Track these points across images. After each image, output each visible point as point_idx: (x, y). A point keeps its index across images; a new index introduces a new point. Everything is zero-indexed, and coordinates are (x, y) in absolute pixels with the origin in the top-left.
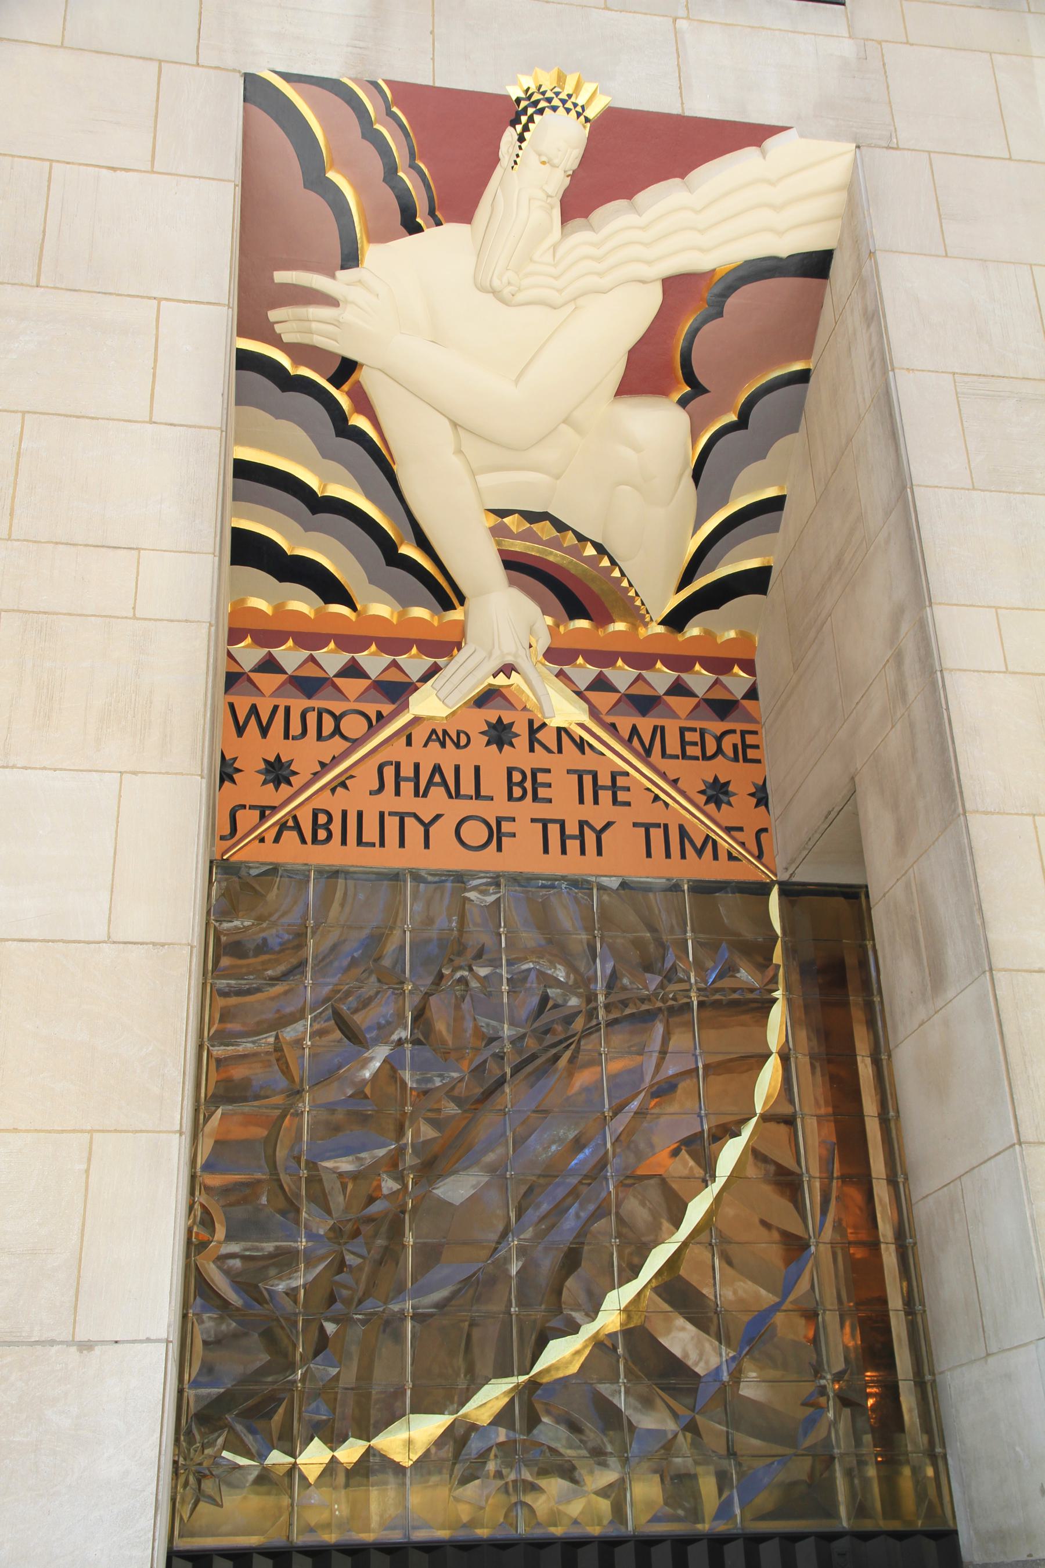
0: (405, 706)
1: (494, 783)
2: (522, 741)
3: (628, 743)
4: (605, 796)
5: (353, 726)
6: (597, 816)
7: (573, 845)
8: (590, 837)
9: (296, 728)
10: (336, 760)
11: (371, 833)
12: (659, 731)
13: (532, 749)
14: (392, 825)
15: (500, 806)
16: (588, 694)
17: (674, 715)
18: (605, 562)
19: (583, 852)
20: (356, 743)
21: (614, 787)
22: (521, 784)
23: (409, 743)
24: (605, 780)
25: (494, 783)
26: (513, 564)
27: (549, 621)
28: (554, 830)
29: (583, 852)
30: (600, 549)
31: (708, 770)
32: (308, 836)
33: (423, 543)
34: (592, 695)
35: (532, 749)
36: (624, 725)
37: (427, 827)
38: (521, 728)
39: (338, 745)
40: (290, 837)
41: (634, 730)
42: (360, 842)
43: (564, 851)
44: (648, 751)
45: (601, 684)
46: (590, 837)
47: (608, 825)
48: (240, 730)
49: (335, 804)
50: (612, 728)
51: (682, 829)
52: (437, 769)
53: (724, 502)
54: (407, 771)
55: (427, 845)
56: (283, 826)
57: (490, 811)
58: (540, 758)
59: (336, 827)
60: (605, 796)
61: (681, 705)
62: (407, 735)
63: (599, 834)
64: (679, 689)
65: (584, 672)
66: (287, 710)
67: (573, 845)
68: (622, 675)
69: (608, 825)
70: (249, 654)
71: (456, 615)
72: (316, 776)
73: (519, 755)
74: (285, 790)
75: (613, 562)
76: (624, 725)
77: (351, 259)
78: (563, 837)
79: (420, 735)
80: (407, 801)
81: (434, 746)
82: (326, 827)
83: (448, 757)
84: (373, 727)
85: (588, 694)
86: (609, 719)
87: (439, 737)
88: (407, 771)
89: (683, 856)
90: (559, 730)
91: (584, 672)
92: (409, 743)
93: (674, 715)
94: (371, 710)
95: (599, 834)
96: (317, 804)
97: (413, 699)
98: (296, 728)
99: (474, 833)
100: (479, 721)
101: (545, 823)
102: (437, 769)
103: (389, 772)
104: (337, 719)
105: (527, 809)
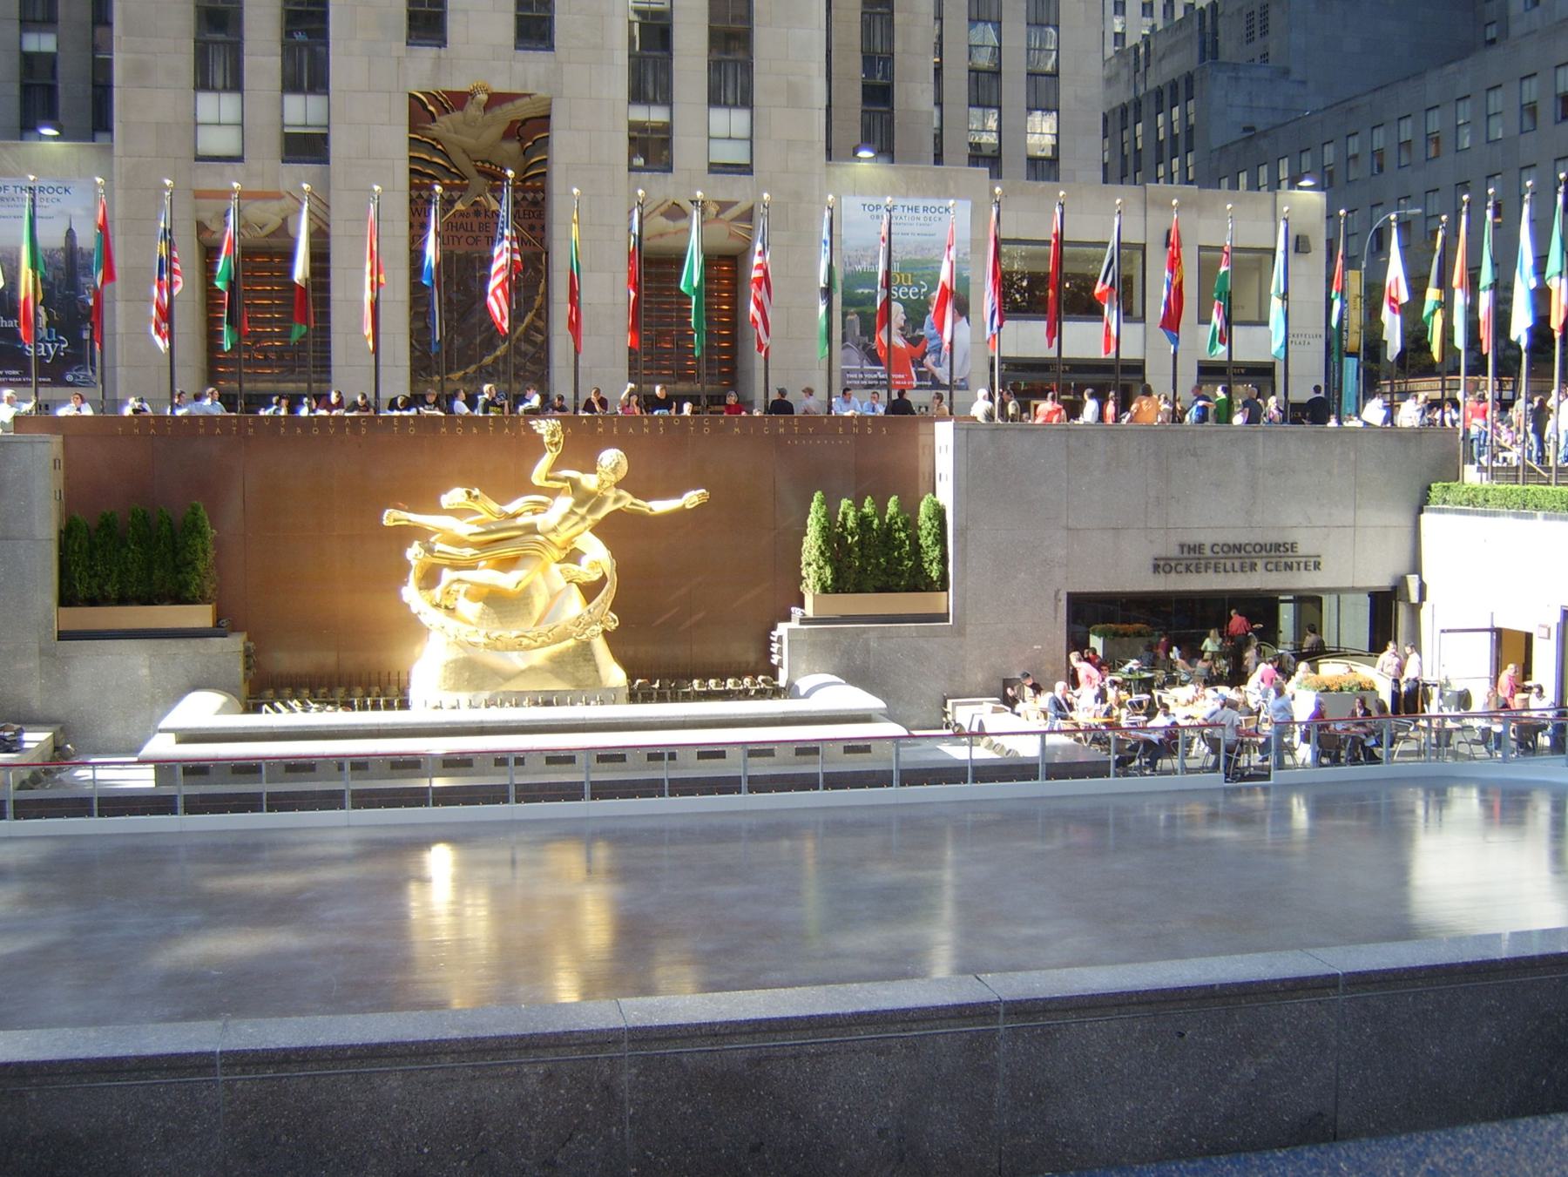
0: (453, 207)
1: (476, 227)
15: (478, 233)
25: (476, 227)
26: (478, 171)
31: (530, 221)
38: (483, 212)
48: (414, 215)
52: (462, 224)
53: (532, 158)
57: (474, 235)
61: (524, 203)
64: (524, 198)
70: (415, 194)
73: (482, 219)
77: (434, 120)
83: (465, 220)
87: (462, 214)
99: (470, 240)
100: (472, 210)
102: (462, 224)
105: (483, 234)
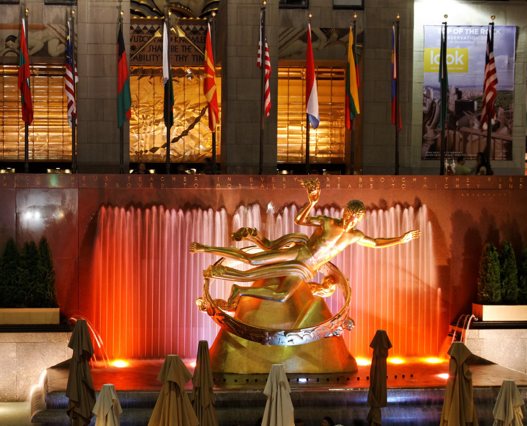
2: (173, 41)
3: (191, 41)
4: (187, 50)
5: (145, 39)
6: (185, 54)
7: (181, 60)
8: (184, 58)
9: (136, 40)
10: (143, 46)
11: (148, 59)
12: (197, 37)
13: (175, 42)
14: (152, 57)
16: (186, 31)
17: (200, 34)
18: (189, 10)
19: (183, 61)
20: (146, 42)
21: (189, 49)
22: (173, 49)
23: (155, 42)
24: (187, 47)
27: (179, 18)
28: (178, 57)
29: (183, 61)
30: (188, 8)
32: (138, 59)
33: (157, 7)
34: (186, 31)
35: (175, 42)
36: (191, 37)
37: (157, 57)
38: (173, 38)
39: (143, 43)
40: (136, 60)
41: (193, 38)
42: (147, 60)
43: (180, 61)
44: (195, 42)
45: (188, 29)
46: (184, 58)
47: (188, 56)
49: (142, 54)
50: (189, 38)
51: (200, 56)
54: (154, 47)
55: (157, 60)
56: (134, 58)
58: (177, 44)
59: (143, 58)
60: (187, 50)
62: (154, 40)
63: (186, 57)
65: (185, 27)
66: (135, 36)
67: (181, 60)
68: (191, 27)
69: (188, 56)
71: (163, 18)
72: (140, 49)
74: (135, 51)
75: (190, 10)
76: (191, 37)
78: (180, 58)
79: (156, 41)
80: (154, 53)
81: (159, 42)
82: (141, 58)
84: (149, 39)
85: (186, 31)
86: (189, 36)
88: (154, 47)
89: (200, 61)
90: (181, 38)
91: (185, 27)
92: (155, 42)
93: (200, 34)
94: (148, 36)
95: (186, 57)
96: (140, 54)
97: (156, 33)
98: (136, 40)
101: (177, 56)
103: (151, 47)
104: (143, 38)
